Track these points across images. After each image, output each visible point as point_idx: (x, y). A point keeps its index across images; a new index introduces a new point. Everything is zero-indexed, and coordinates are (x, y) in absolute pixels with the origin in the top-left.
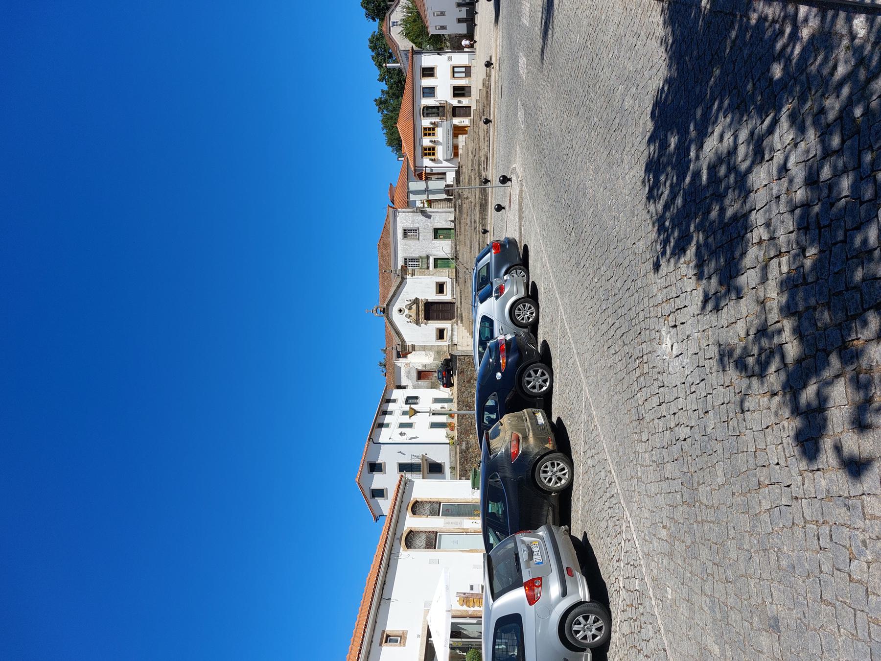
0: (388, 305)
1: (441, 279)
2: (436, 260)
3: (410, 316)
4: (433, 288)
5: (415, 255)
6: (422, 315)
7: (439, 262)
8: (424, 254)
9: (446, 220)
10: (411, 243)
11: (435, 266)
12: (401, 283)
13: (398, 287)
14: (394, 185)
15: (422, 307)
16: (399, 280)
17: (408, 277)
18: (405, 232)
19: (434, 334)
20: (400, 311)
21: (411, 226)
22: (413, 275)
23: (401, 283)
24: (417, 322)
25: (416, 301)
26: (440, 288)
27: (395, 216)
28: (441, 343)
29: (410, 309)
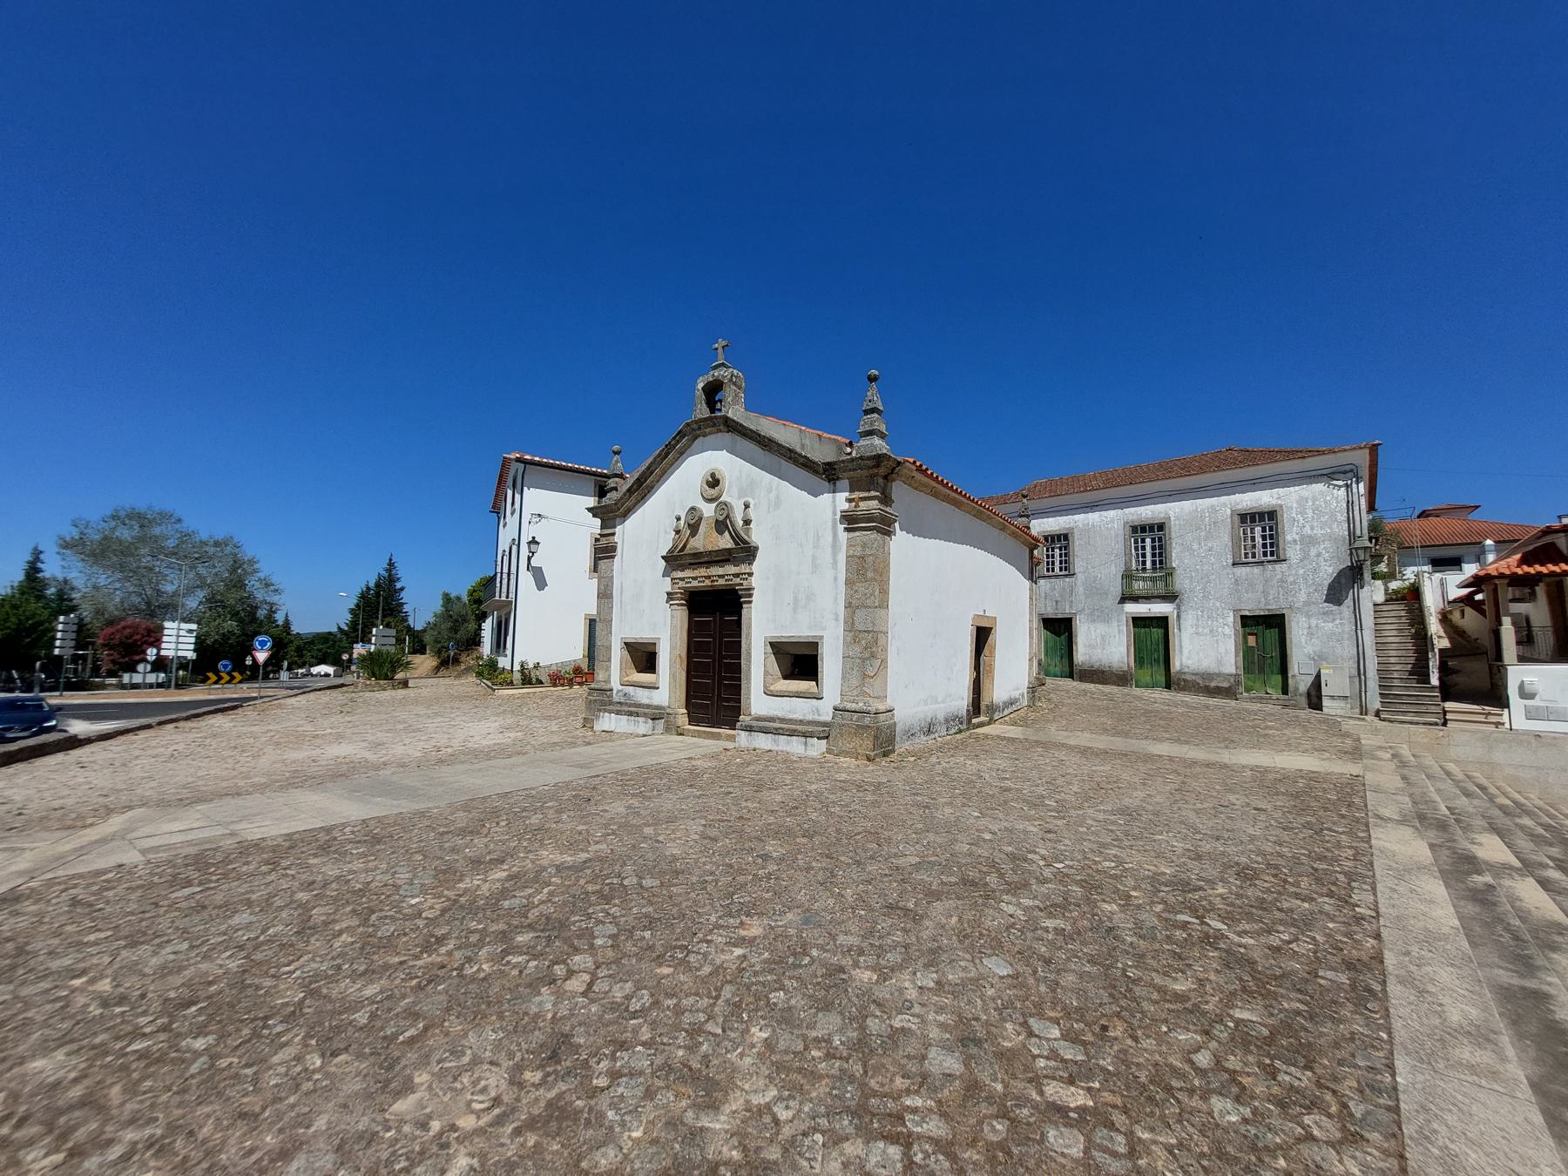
0: (731, 426)
1: (831, 665)
2: (1162, 622)
3: (694, 528)
4: (796, 630)
5: (1178, 557)
6: (698, 578)
7: (1157, 633)
8: (1181, 582)
9: (1319, 658)
10: (1223, 541)
11: (1138, 621)
12: (807, 464)
13: (791, 455)
14: (1474, 516)
15: (721, 575)
16: (821, 453)
17: (841, 500)
18: (1268, 518)
19: (641, 634)
20: (714, 482)
21: (1290, 534)
22: (851, 521)
23: (807, 464)
24: (674, 560)
25: (744, 552)
26: (800, 662)
27: (1329, 476)
28: (617, 654)
29: (722, 525)
